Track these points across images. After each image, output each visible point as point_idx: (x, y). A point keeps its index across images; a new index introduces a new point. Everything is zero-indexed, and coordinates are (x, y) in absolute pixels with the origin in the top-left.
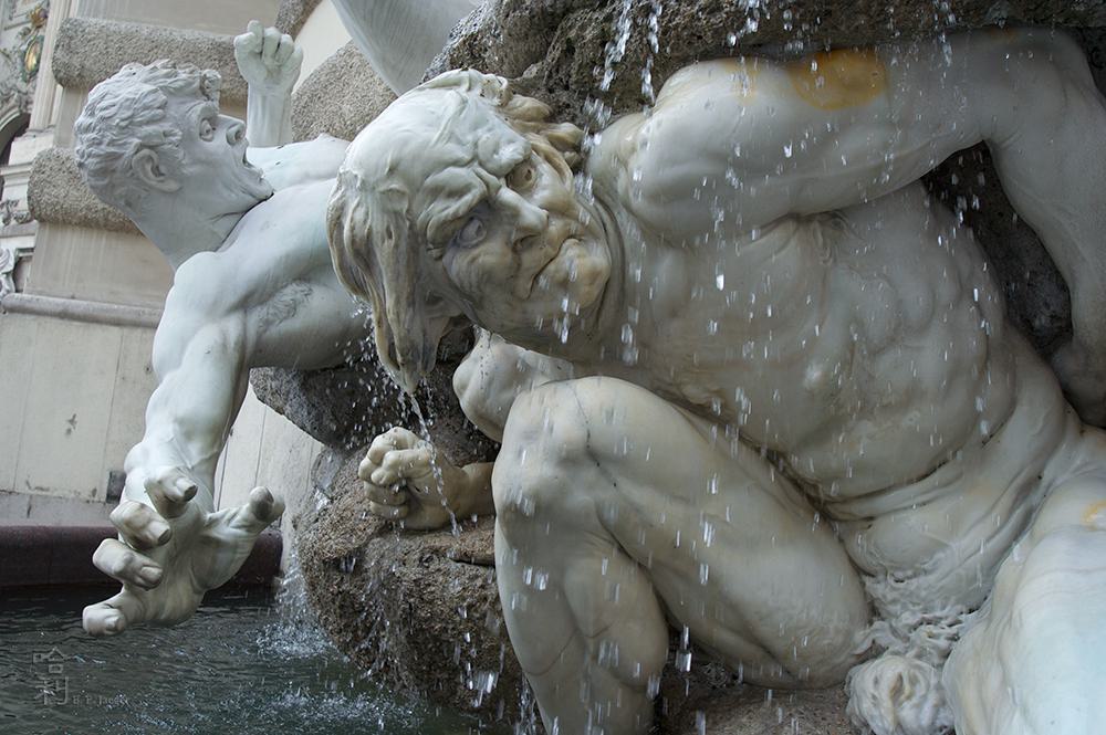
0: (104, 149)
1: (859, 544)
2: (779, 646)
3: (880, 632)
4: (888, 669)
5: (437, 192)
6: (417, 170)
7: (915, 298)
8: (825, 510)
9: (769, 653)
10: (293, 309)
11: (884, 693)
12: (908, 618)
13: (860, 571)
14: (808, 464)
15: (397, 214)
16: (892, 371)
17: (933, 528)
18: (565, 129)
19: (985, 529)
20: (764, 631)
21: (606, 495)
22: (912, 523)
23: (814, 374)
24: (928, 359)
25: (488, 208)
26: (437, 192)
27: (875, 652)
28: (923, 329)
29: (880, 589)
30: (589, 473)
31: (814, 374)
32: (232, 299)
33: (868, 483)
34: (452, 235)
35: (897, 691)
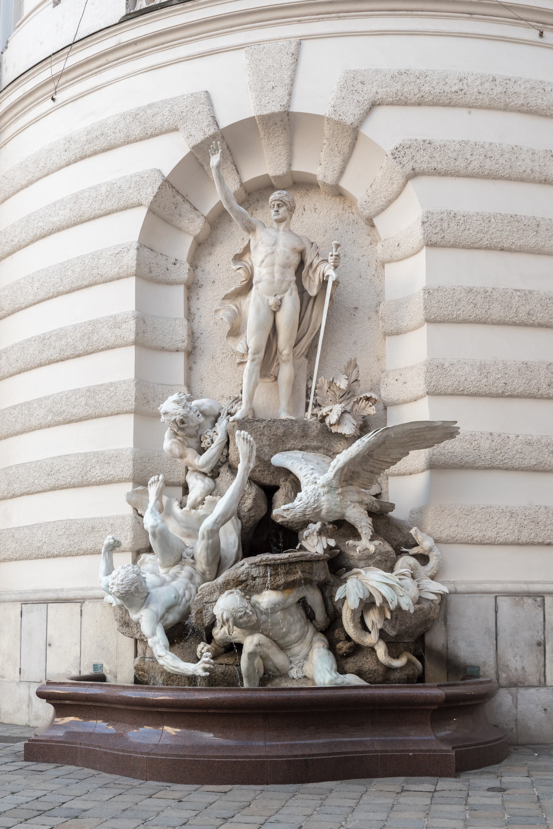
0: (127, 589)
1: (289, 653)
2: (280, 669)
3: (293, 665)
4: (295, 670)
5: (239, 612)
6: (236, 609)
7: (296, 618)
8: (283, 648)
9: (278, 670)
10: (166, 619)
11: (295, 673)
12: (297, 662)
13: (289, 657)
14: (281, 642)
15: (233, 615)
16: (293, 628)
17: (299, 649)
18: (248, 597)
19: (306, 649)
20: (278, 666)
21: (261, 650)
22: (296, 649)
23: (284, 630)
24: (298, 626)
25: (246, 613)
26: (239, 612)
27: (292, 668)
28: (297, 622)
29: (292, 659)
30: (259, 647)
31: (284, 630)
32: (159, 619)
33: (290, 644)
34: (241, 617)
35: (297, 672)
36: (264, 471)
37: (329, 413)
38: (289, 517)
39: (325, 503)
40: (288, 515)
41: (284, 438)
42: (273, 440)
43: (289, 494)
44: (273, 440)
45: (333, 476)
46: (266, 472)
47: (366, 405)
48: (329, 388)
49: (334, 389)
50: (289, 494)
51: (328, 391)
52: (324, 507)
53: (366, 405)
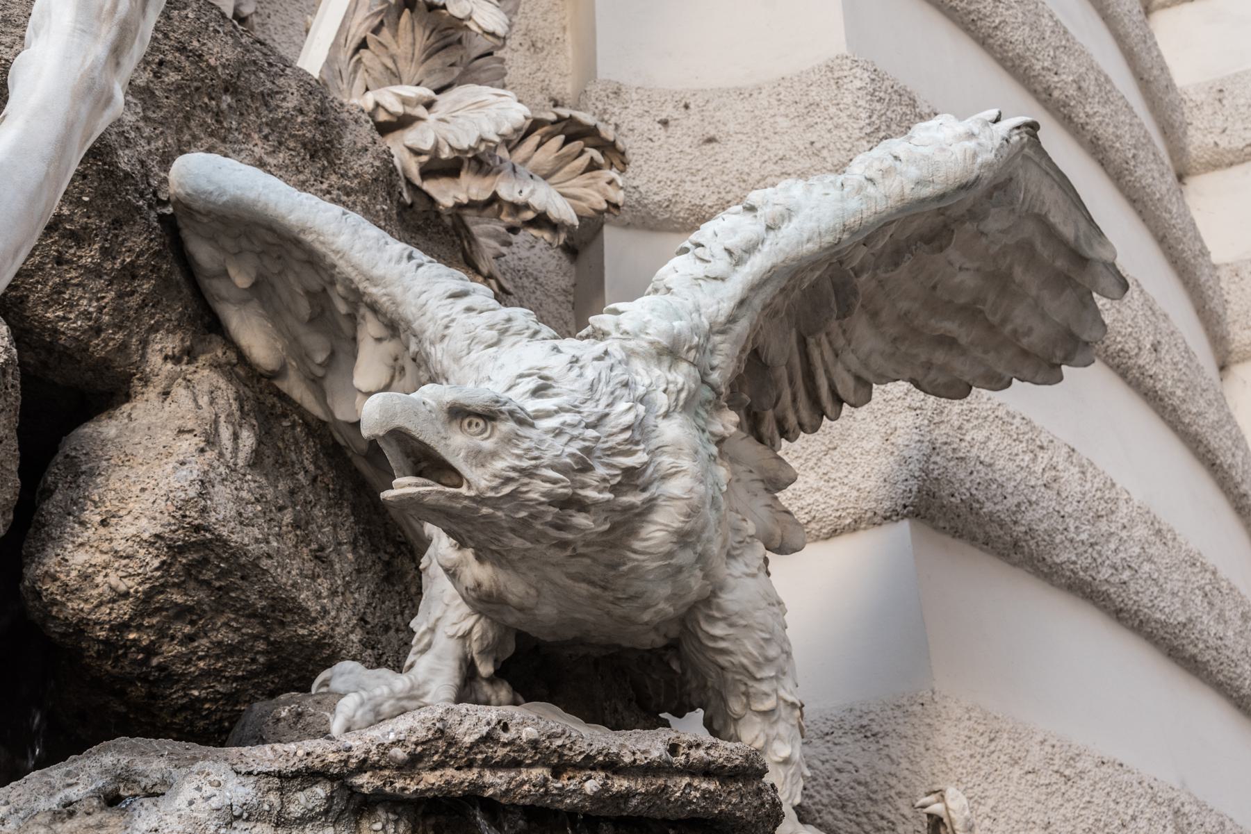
36: (79, 238)
37: (420, 111)
38: (479, 479)
39: (686, 463)
40: (479, 457)
41: (227, 99)
42: (173, 77)
43: (225, 433)
44: (173, 77)
45: (727, 307)
46: (89, 255)
47: (562, 161)
48: (376, 31)
49: (393, 48)
50: (225, 433)
51: (363, 44)
52: (675, 487)
53: (562, 161)
